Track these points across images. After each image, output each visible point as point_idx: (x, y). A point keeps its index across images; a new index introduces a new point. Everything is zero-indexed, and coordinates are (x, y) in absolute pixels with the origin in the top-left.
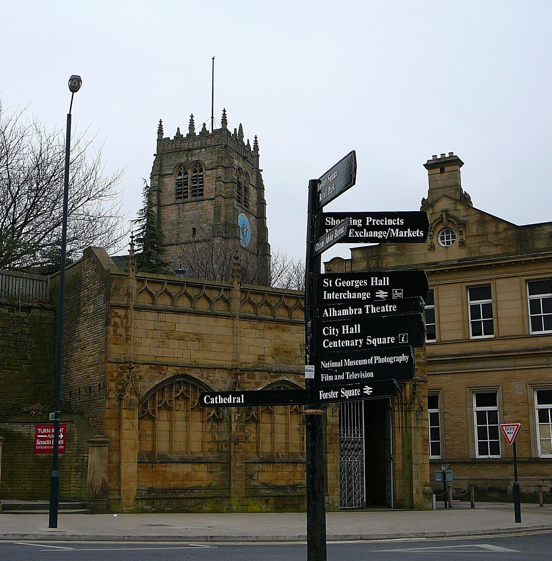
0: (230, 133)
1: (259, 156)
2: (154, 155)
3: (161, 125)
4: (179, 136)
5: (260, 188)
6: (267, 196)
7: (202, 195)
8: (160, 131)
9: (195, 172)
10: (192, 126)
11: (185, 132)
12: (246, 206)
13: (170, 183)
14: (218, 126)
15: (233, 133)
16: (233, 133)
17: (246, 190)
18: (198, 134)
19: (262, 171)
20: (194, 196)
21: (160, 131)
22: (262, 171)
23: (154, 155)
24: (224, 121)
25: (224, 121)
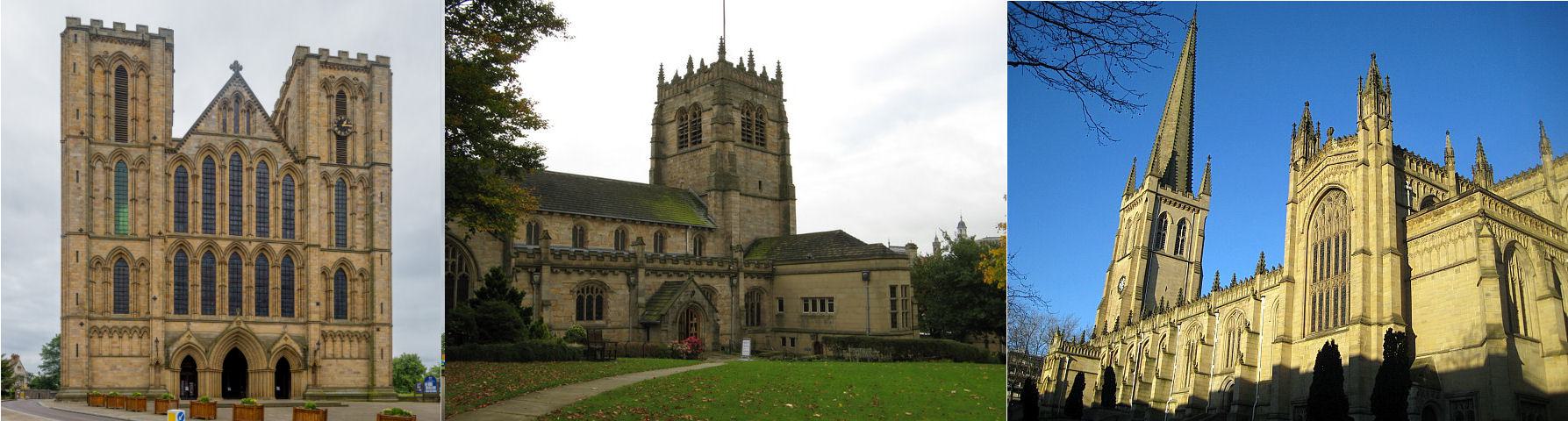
0: (732, 64)
1: (782, 83)
2: (656, 103)
3: (661, 69)
4: (677, 78)
5: (782, 120)
6: (792, 129)
7: (700, 142)
8: (661, 76)
9: (695, 116)
10: (690, 65)
11: (683, 73)
12: (762, 145)
13: (672, 131)
14: (711, 58)
15: (736, 64)
16: (736, 64)
17: (761, 125)
18: (695, 72)
19: (785, 100)
20: (695, 144)
21: (661, 76)
22: (785, 100)
23: (656, 103)
24: (722, 50)
25: (722, 50)
